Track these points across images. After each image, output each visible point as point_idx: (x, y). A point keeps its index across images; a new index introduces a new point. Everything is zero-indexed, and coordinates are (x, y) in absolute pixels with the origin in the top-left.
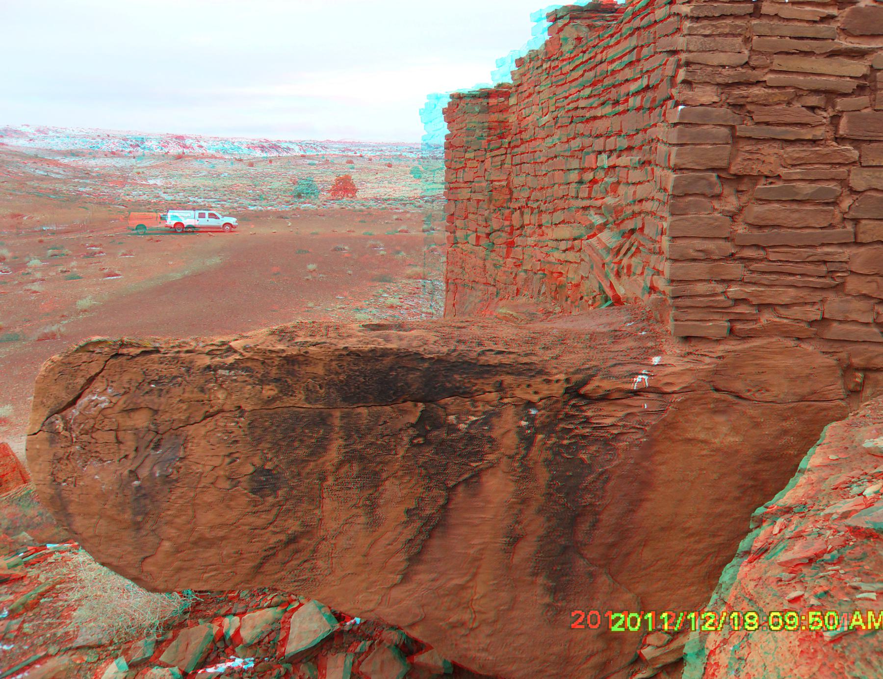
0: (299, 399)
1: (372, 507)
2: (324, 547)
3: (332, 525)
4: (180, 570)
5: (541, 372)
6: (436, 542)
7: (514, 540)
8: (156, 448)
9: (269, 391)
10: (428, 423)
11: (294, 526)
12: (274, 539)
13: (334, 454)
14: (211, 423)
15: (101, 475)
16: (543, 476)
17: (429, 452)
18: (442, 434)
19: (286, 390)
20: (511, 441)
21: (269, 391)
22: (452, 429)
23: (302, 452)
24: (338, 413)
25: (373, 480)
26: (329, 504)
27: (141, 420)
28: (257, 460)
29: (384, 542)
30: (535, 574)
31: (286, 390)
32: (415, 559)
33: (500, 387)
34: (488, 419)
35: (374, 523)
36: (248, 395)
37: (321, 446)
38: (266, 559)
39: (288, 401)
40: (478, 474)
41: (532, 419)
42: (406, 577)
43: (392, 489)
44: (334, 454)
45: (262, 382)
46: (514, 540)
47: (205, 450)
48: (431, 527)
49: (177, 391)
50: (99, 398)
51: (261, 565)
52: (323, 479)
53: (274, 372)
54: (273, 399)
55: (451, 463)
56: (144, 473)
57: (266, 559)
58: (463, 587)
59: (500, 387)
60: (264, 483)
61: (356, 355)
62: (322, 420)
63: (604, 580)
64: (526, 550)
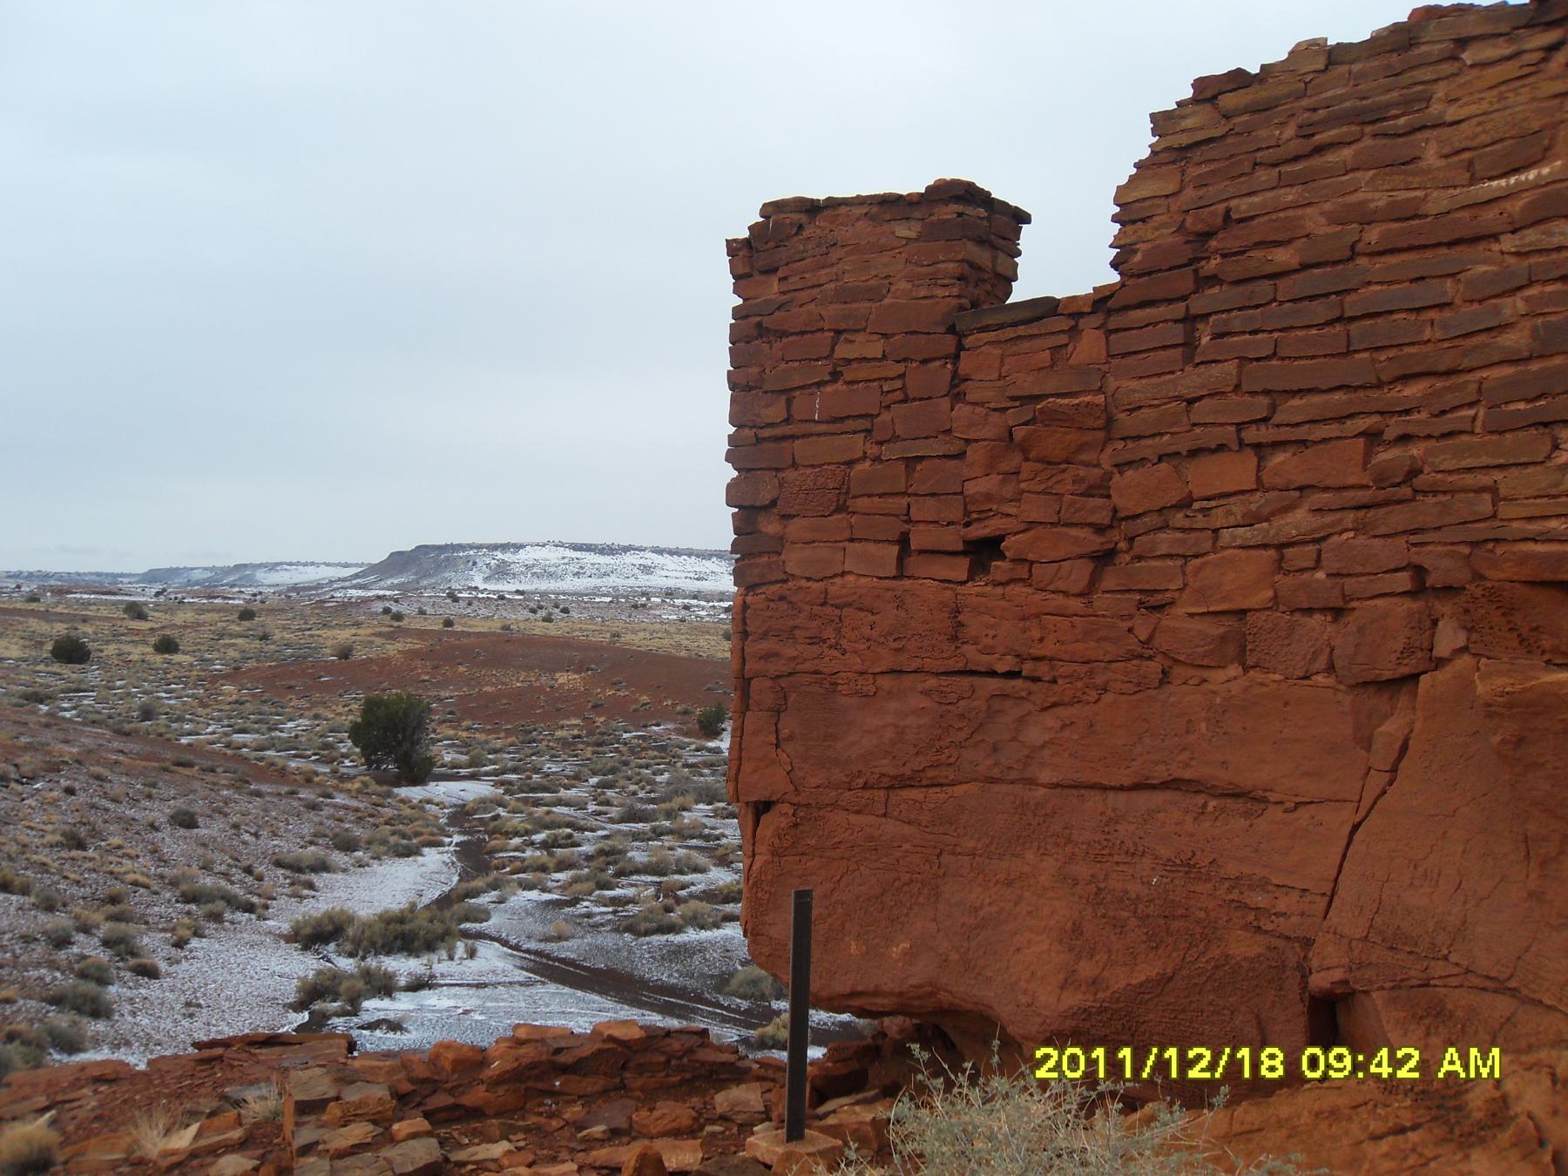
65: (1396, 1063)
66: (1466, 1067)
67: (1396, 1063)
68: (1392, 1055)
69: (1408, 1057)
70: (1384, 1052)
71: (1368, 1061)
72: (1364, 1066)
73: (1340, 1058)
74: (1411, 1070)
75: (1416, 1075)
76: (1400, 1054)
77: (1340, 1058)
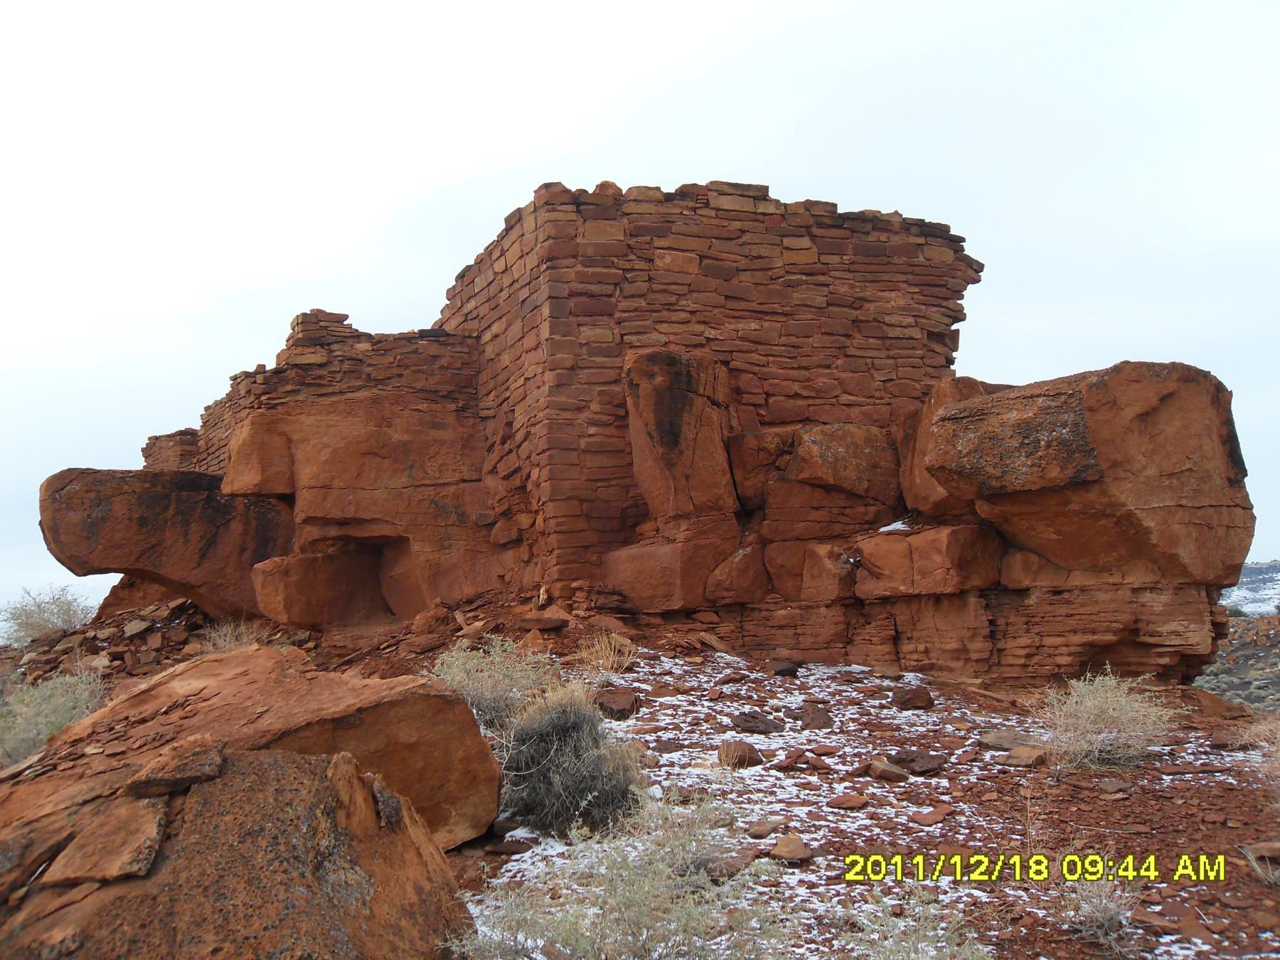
0: (159, 488)
1: (186, 534)
2: (165, 552)
3: (169, 543)
7: (243, 550)
9: (147, 485)
11: (154, 541)
13: (171, 511)
16: (254, 523)
17: (209, 511)
18: (215, 504)
19: (154, 485)
20: (241, 508)
21: (147, 485)
22: (219, 502)
23: (158, 510)
25: (186, 523)
26: (167, 534)
27: (92, 495)
31: (154, 485)
32: (203, 557)
36: (138, 487)
42: (199, 565)
43: (194, 527)
44: (171, 511)
46: (243, 550)
47: (119, 508)
56: (94, 515)
58: (221, 569)
60: (143, 522)
62: (167, 497)
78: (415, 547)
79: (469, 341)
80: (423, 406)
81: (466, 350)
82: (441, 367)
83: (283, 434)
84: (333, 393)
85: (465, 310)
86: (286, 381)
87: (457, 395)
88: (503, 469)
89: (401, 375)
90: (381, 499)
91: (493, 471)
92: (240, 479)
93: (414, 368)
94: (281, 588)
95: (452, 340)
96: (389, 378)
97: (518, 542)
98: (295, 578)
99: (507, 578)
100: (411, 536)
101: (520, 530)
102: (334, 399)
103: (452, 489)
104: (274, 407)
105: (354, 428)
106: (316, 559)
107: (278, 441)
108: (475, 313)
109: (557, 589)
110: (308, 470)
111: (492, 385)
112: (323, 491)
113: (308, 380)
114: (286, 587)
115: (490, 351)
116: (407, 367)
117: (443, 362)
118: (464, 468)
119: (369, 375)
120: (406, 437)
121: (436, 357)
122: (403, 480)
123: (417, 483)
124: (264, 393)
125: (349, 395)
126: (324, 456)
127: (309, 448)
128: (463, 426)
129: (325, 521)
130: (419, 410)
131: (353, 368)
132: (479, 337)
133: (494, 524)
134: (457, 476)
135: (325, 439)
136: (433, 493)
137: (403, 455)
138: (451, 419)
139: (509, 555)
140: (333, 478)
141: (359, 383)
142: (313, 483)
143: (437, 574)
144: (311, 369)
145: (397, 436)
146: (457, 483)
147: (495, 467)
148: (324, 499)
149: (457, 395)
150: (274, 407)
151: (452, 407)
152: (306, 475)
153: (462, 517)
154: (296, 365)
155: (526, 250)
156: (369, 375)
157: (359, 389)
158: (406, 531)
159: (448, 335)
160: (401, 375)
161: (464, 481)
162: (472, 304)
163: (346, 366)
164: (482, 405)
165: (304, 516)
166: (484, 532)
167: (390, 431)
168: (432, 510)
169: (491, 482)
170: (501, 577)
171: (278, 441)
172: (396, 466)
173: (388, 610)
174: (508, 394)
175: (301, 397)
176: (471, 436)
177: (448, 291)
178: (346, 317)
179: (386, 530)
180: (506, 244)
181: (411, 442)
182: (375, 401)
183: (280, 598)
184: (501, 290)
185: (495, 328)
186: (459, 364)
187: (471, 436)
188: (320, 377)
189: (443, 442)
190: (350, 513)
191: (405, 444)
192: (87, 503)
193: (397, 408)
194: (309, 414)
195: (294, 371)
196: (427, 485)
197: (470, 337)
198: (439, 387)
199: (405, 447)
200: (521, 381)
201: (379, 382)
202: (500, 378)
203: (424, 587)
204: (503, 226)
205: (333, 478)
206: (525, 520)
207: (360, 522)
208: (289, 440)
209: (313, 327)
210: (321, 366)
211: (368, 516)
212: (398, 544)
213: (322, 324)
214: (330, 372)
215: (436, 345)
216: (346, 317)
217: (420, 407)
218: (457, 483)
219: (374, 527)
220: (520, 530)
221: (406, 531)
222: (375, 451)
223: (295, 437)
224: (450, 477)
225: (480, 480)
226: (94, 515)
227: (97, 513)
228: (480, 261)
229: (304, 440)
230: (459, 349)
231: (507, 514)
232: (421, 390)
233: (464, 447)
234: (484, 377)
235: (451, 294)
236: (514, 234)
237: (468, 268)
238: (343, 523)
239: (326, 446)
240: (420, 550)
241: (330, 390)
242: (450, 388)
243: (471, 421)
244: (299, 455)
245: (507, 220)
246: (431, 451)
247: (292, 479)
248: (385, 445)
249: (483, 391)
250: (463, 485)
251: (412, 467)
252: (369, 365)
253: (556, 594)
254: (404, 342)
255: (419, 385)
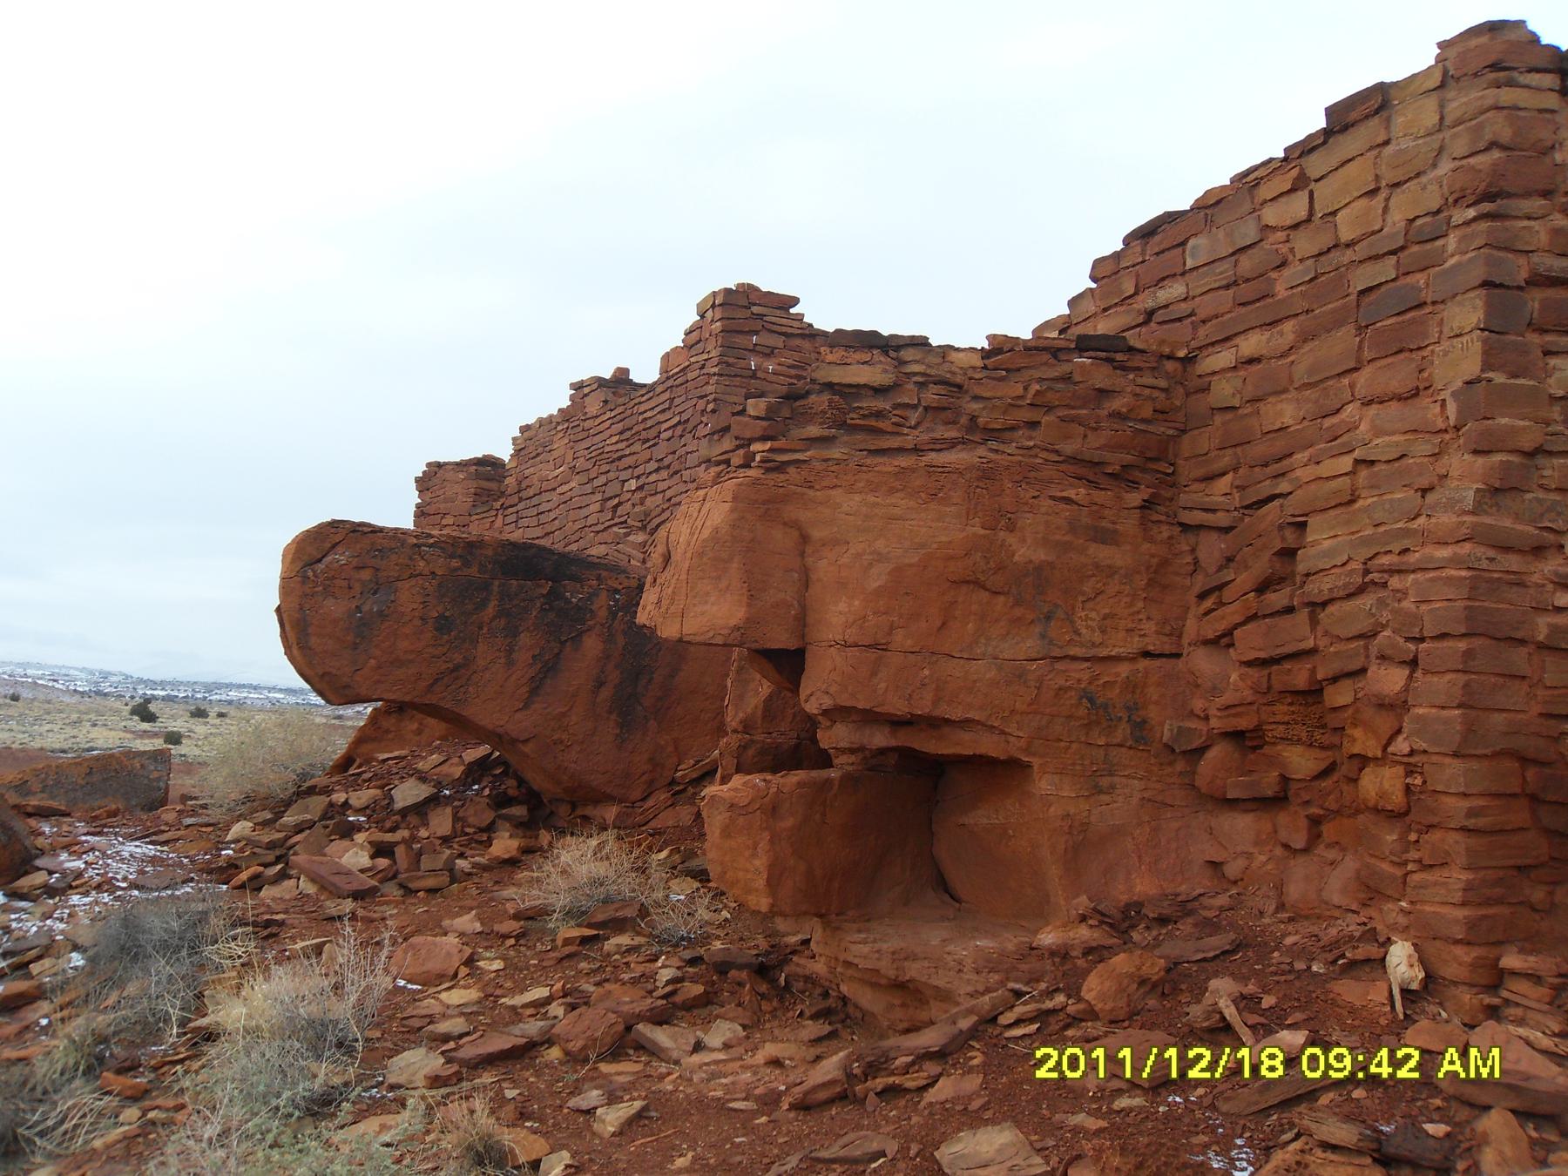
1: (510, 651)
3: (481, 662)
4: (378, 682)
5: (624, 572)
6: (548, 681)
7: (601, 684)
8: (375, 593)
9: (455, 563)
10: (553, 595)
11: (458, 658)
12: (444, 667)
13: (491, 609)
14: (413, 582)
15: (335, 607)
17: (551, 615)
19: (467, 564)
20: (603, 613)
21: (455, 563)
22: (568, 601)
24: (497, 583)
25: (513, 632)
26: (481, 647)
27: (366, 575)
28: (440, 609)
29: (514, 678)
30: (610, 713)
31: (467, 564)
32: (534, 692)
33: (599, 578)
34: (591, 596)
35: (510, 663)
36: (440, 565)
37: (483, 604)
38: (437, 680)
39: (466, 571)
40: (580, 634)
41: (616, 601)
42: (526, 707)
43: (525, 639)
44: (491, 609)
45: (452, 556)
47: (408, 597)
48: (548, 668)
49: (394, 557)
50: (341, 557)
51: (432, 685)
52: (481, 628)
53: (459, 551)
54: (456, 569)
55: (566, 623)
56: (366, 608)
57: (437, 680)
58: (563, 715)
59: (599, 578)
60: (443, 625)
61: (514, 545)
63: (652, 724)
64: (605, 693)
65: (1396, 1064)
66: (1467, 1070)
67: (1396, 1064)
68: (1392, 1053)
69: (1408, 1057)
70: (1384, 1052)
71: (1368, 1061)
72: (1365, 1068)
73: (1340, 1058)
74: (1411, 1070)
75: (1416, 1075)
76: (1400, 1054)
77: (1340, 1058)
78: (1044, 784)
79: (1170, 366)
80: (1078, 493)
81: (1163, 383)
82: (1116, 415)
83: (795, 525)
84: (901, 450)
85: (1147, 301)
86: (807, 417)
87: (1137, 474)
88: (1252, 642)
89: (1034, 425)
90: (982, 677)
91: (1223, 641)
92: (691, 602)
93: (1062, 412)
94: (763, 845)
95: (1137, 361)
96: (1012, 429)
97: (1277, 801)
98: (789, 822)
99: (1232, 870)
100: (1036, 762)
101: (1285, 780)
102: (904, 461)
103: (1124, 670)
104: (781, 468)
105: (942, 527)
106: (828, 781)
107: (781, 538)
108: (1185, 308)
109: (1457, 962)
110: (842, 606)
111: (1226, 459)
112: (872, 655)
113: (853, 418)
114: (771, 841)
115: (1224, 391)
116: (1050, 409)
117: (1117, 404)
118: (1149, 627)
119: (973, 419)
120: (1041, 555)
121: (1103, 393)
122: (1029, 644)
123: (1057, 652)
124: (764, 439)
125: (932, 457)
126: (878, 578)
127: (845, 560)
128: (1151, 540)
129: (869, 717)
130: (1067, 500)
131: (944, 401)
132: (1189, 360)
133: (1201, 751)
134: (1136, 644)
135: (880, 545)
136: (1086, 676)
137: (1036, 593)
138: (1129, 524)
139: (1241, 826)
140: (892, 628)
141: (952, 433)
142: (852, 635)
143: (1082, 845)
144: (857, 396)
145: (1025, 551)
146: (1132, 659)
147: (1229, 633)
148: (874, 673)
149: (1137, 474)
150: (781, 468)
151: (1135, 498)
152: (837, 616)
153: (1141, 730)
154: (830, 386)
155: (1389, 176)
156: (973, 419)
157: (952, 444)
158: (1027, 751)
159: (1131, 349)
160: (1034, 425)
161: (1147, 654)
162: (1176, 290)
163: (931, 396)
164: (1184, 499)
165: (827, 702)
166: (1180, 766)
167: (1012, 540)
168: (1082, 712)
169: (1203, 663)
170: (1215, 865)
171: (781, 538)
172: (1018, 612)
173: (943, 885)
174: (1284, 486)
175: (836, 453)
176: (1165, 563)
177: (1098, 263)
178: (795, 301)
179: (988, 745)
180: (1316, 165)
181: (1051, 565)
182: (987, 474)
183: (761, 863)
184: (1283, 264)
185: (1250, 344)
186: (1147, 412)
187: (1165, 563)
188: (879, 414)
189: (1111, 571)
190: (923, 706)
191: (1039, 568)
192: (357, 588)
193: (1027, 493)
194: (851, 489)
195: (826, 397)
196: (1074, 658)
197: (1169, 357)
198: (1107, 456)
199: (1039, 576)
200: (1346, 463)
201: (991, 434)
202: (1260, 449)
203: (1054, 872)
204: (1321, 123)
205: (892, 628)
206: (1301, 761)
207: (934, 723)
208: (805, 539)
209: (740, 314)
210: (879, 391)
211: (956, 713)
212: (1002, 773)
213: (755, 309)
214: (896, 406)
215: (1106, 369)
216: (795, 301)
217: (1070, 493)
218: (1132, 659)
219: (966, 736)
220: (1285, 780)
221: (1027, 751)
222: (978, 579)
223: (816, 534)
224: (1121, 645)
225: (1178, 656)
226: (366, 608)
227: (371, 606)
228: (1211, 206)
229: (835, 542)
230: (1150, 381)
231: (1246, 740)
232: (1073, 459)
233: (1151, 583)
234: (1204, 440)
235: (1104, 270)
236: (1350, 144)
237: (1170, 218)
238: (899, 723)
239: (880, 558)
240: (1052, 790)
241: (894, 442)
242: (1128, 458)
243: (1166, 532)
244: (823, 568)
245: (1330, 112)
246: (1088, 587)
247: (802, 622)
248: (1000, 568)
249: (1188, 471)
250: (1143, 664)
251: (1048, 618)
252: (976, 398)
253: (1449, 971)
254: (1046, 357)
255: (1069, 448)
